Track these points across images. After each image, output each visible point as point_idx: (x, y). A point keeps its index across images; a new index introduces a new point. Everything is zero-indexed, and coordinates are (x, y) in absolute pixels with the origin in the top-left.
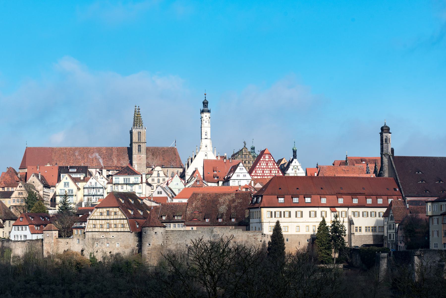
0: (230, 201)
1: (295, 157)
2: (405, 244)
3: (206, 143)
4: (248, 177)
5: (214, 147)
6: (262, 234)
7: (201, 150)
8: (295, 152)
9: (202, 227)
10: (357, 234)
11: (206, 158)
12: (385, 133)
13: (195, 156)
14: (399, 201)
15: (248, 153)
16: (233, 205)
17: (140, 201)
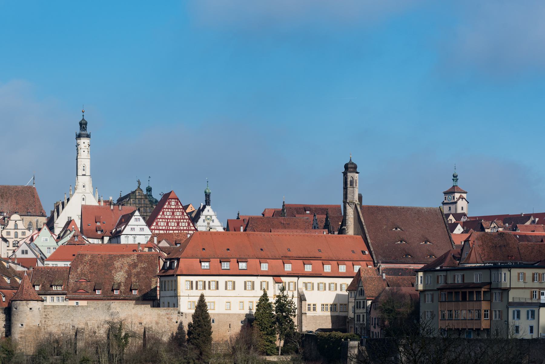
0: (130, 266)
1: (208, 203)
2: (381, 329)
3: (84, 181)
4: (147, 231)
5: (95, 187)
6: (179, 313)
7: (76, 191)
8: (207, 196)
9: (95, 302)
10: (310, 314)
11: (83, 203)
12: (351, 172)
13: (68, 200)
14: (370, 268)
15: (143, 197)
16: (134, 271)
17: (5, 264)
